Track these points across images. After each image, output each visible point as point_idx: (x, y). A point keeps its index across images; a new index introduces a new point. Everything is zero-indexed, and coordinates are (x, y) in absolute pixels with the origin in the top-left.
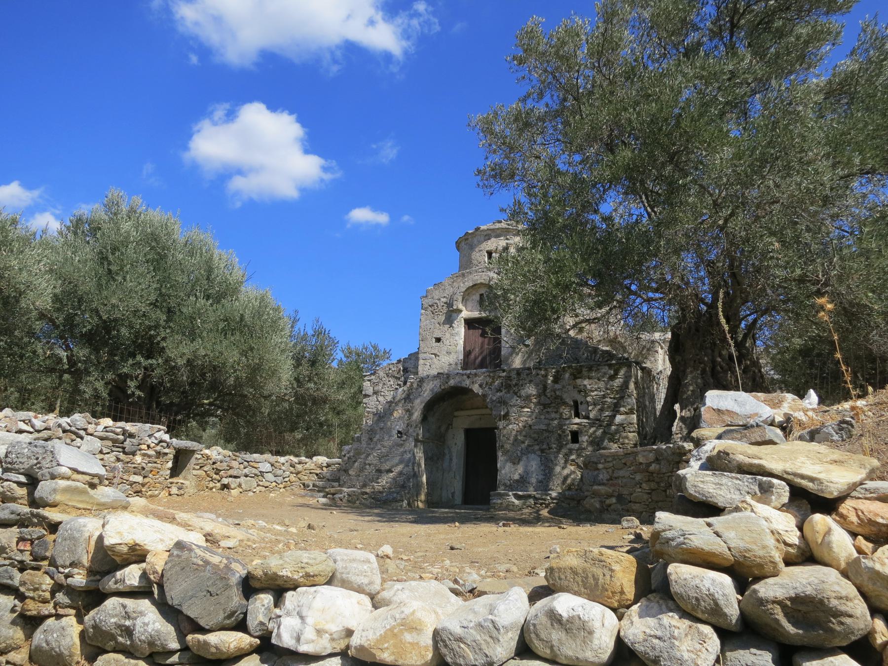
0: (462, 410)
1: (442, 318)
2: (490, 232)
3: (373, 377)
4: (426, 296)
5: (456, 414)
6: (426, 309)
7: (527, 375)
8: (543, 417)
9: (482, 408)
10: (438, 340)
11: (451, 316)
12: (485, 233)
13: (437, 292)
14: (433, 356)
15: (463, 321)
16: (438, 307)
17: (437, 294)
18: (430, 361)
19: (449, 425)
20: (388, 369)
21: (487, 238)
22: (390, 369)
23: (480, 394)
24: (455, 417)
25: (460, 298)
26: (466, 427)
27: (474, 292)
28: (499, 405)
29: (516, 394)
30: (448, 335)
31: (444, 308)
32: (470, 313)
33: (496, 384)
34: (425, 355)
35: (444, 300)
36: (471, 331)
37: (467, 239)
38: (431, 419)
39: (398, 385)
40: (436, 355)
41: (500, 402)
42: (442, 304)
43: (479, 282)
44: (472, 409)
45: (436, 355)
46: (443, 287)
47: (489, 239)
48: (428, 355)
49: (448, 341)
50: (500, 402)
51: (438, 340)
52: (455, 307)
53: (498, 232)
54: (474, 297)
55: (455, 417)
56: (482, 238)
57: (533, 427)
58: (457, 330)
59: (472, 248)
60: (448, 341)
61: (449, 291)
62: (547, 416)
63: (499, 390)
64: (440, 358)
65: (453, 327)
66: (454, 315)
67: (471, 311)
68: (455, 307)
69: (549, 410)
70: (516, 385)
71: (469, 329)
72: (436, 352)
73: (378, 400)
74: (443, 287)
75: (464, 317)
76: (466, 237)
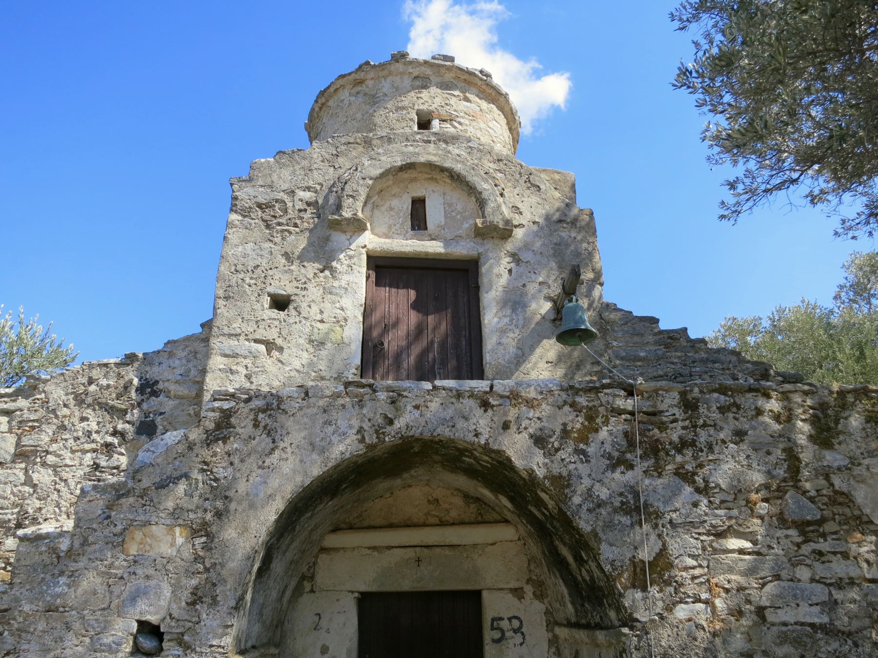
0: (351, 527)
1: (299, 243)
2: (428, 71)
3: (22, 403)
4: (250, 180)
5: (332, 540)
6: (245, 213)
7: (722, 410)
8: (803, 573)
9: (425, 525)
10: (280, 303)
11: (327, 239)
12: (416, 72)
13: (286, 173)
14: (262, 348)
15: (364, 258)
16: (285, 211)
17: (284, 178)
18: (249, 362)
19: (303, 578)
20: (85, 380)
21: (418, 83)
22: (91, 381)
23: (540, 473)
24: (324, 550)
25: (363, 193)
26: (363, 588)
27: (395, 190)
28: (626, 520)
29: (687, 477)
30: (314, 292)
31: (307, 215)
32: (383, 240)
33: (603, 434)
34: (233, 342)
35: (308, 195)
36: (384, 292)
37: (361, 82)
38: (278, 566)
39: (115, 433)
40: (270, 346)
41: (625, 509)
42: (300, 205)
43: (422, 159)
44: (391, 526)
45: (270, 346)
46: (305, 163)
47: (425, 87)
48: (243, 346)
49: (315, 309)
50: (625, 509)
51: (280, 303)
52: (347, 214)
53: (449, 76)
54: (395, 203)
55: (324, 550)
56: (407, 81)
57: (770, 616)
58: (344, 279)
59: (374, 100)
60: (315, 309)
61: (324, 176)
62: (820, 570)
63: (619, 462)
64: (285, 357)
65: (333, 270)
66: (338, 238)
67: (387, 236)
68: (347, 214)
69: (823, 546)
70: (683, 445)
71: (378, 284)
72: (272, 335)
73: (29, 481)
74: (305, 163)
75: (370, 247)
76: (361, 75)
